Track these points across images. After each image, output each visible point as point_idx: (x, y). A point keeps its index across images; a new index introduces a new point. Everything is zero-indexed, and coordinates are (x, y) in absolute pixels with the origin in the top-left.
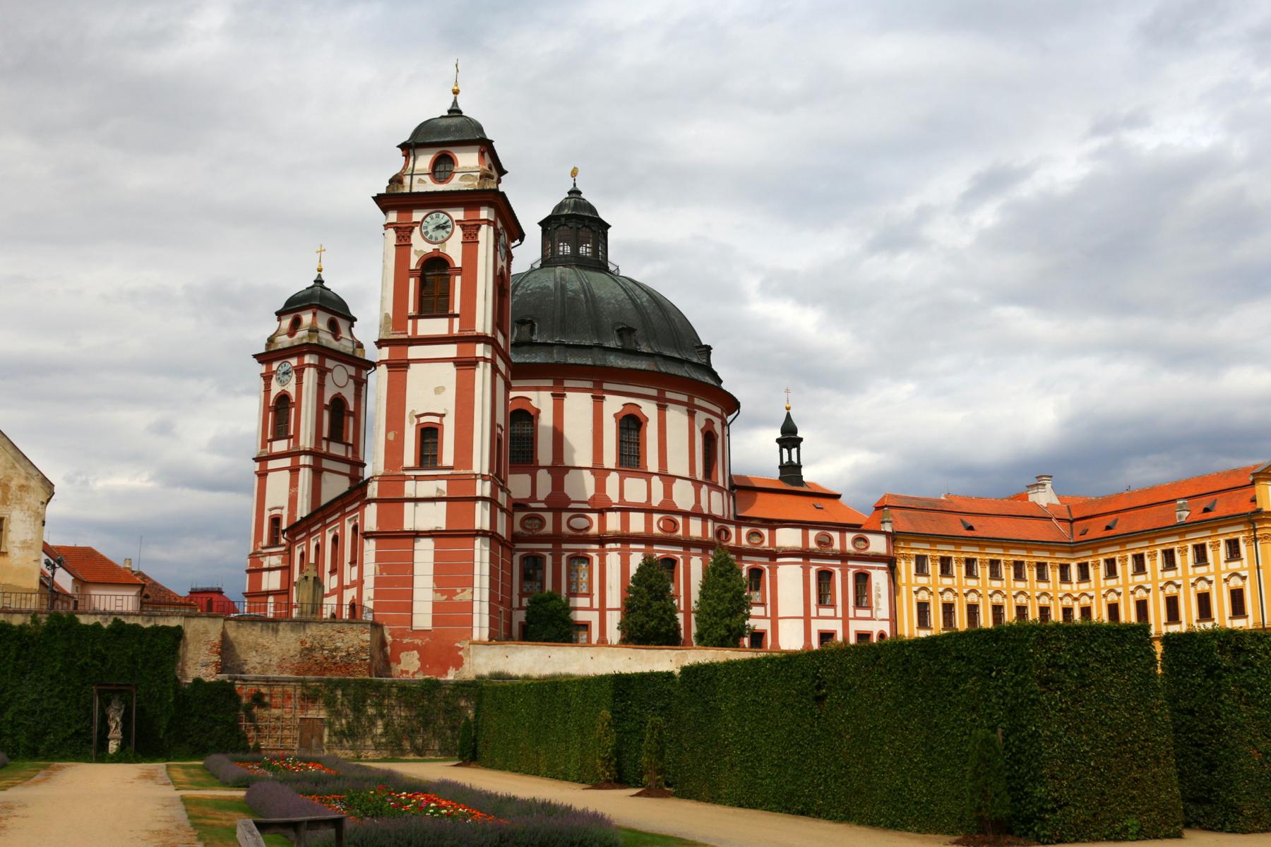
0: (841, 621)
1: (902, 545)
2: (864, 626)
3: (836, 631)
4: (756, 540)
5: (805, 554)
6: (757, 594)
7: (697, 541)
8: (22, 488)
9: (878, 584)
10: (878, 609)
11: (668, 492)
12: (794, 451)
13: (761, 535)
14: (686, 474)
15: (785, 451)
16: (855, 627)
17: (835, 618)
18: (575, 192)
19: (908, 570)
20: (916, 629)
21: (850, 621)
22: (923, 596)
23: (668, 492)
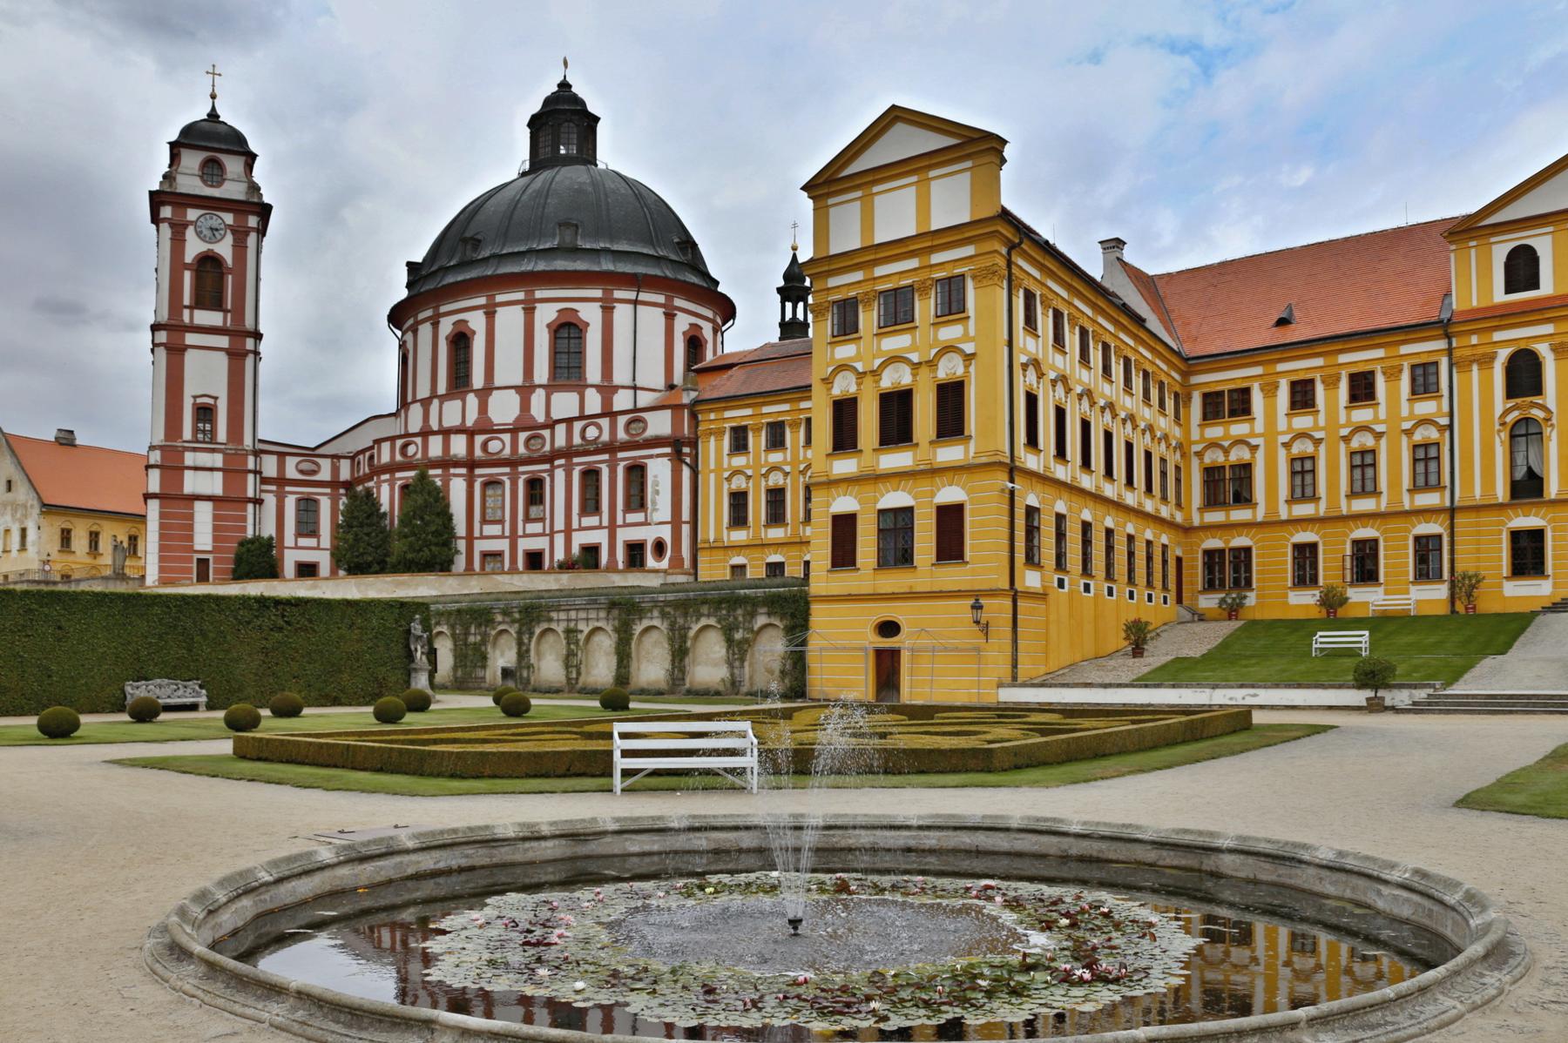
0: (606, 532)
1: (712, 416)
2: (635, 534)
3: (600, 544)
4: (535, 444)
5: (569, 453)
6: (541, 507)
7: (437, 461)
8: (32, 506)
9: (655, 476)
10: (655, 510)
11: (483, 408)
13: (541, 437)
14: (518, 379)
15: (789, 305)
16: (624, 535)
17: (600, 527)
18: (564, 86)
19: (719, 450)
20: (725, 532)
21: (618, 529)
22: (739, 483)
23: (483, 408)
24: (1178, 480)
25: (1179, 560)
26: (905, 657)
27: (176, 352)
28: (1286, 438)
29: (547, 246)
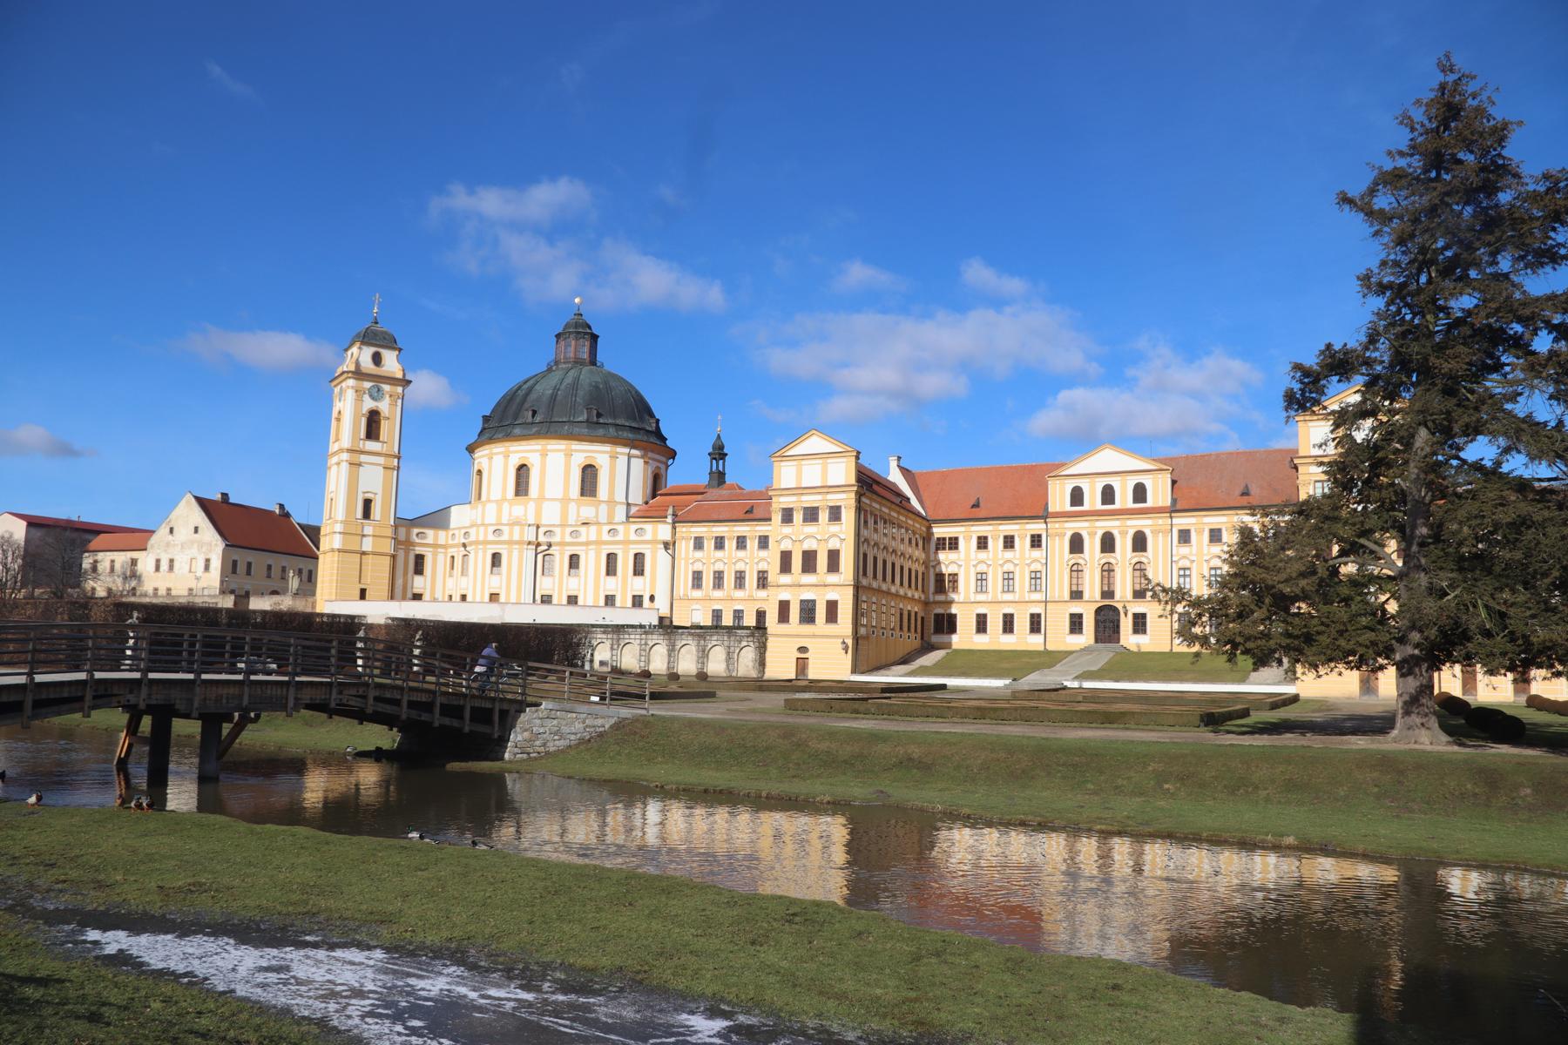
8: (216, 545)
12: (721, 462)
22: (698, 567)
24: (923, 579)
25: (922, 618)
26: (811, 662)
27: (355, 465)
28: (975, 563)
29: (580, 419)
